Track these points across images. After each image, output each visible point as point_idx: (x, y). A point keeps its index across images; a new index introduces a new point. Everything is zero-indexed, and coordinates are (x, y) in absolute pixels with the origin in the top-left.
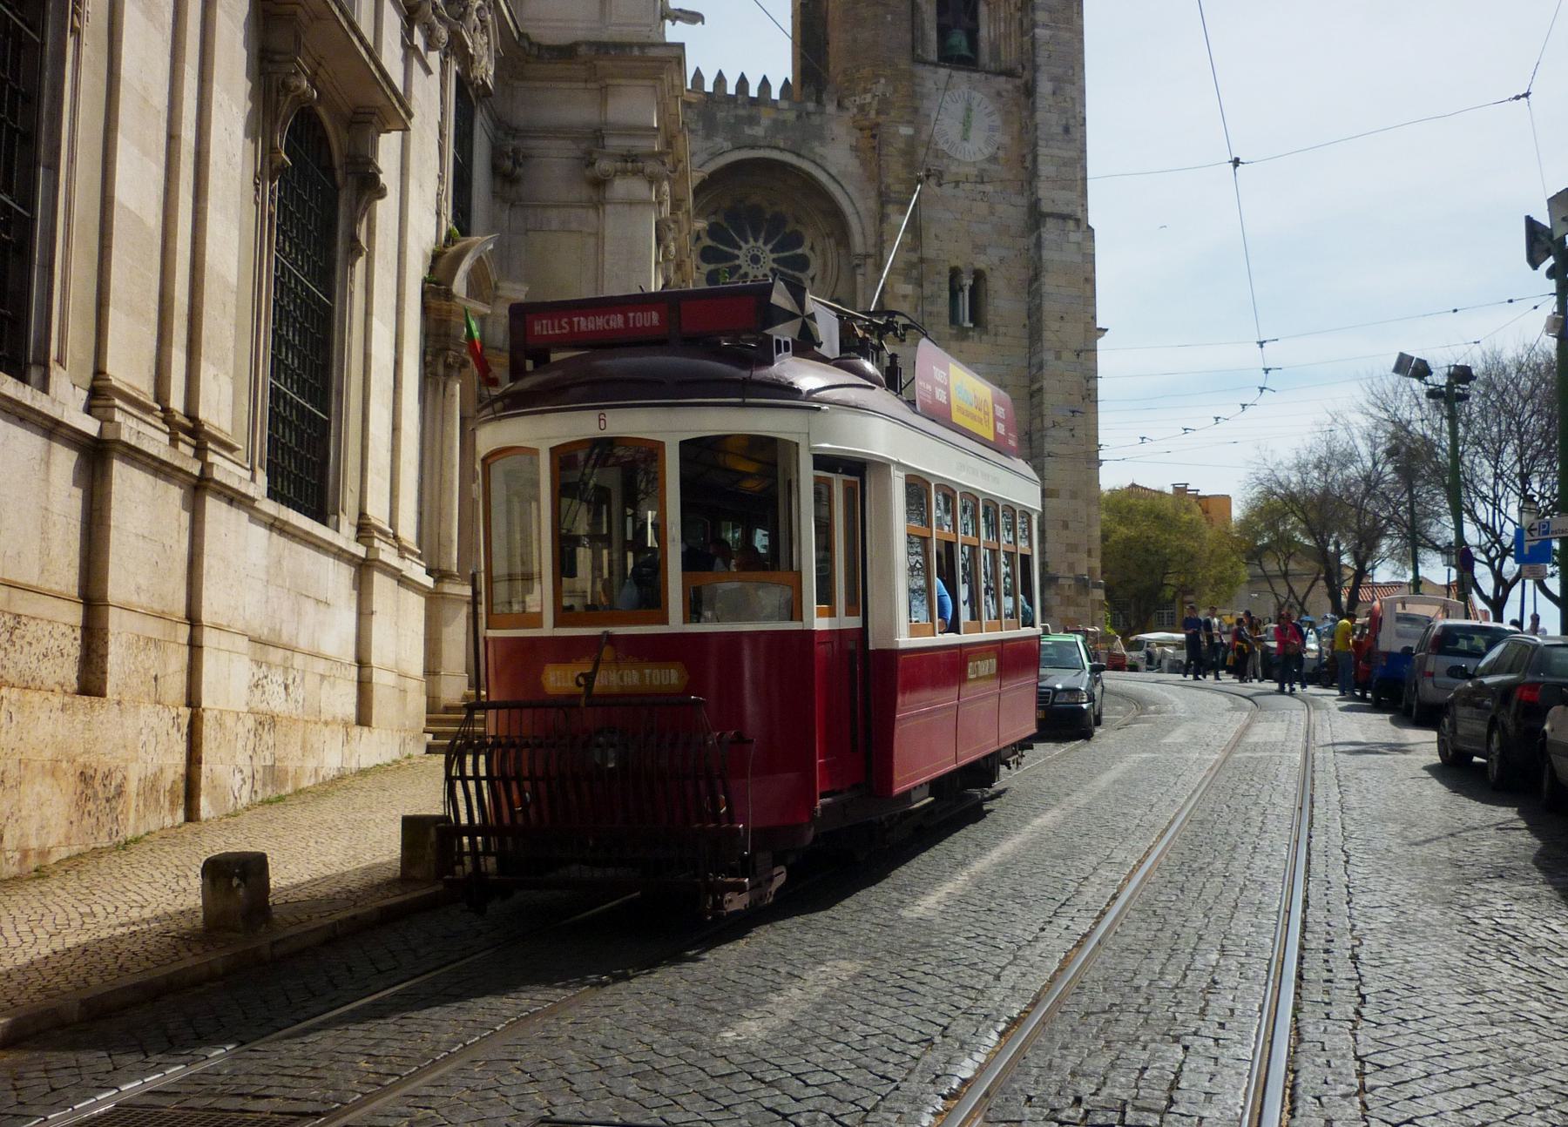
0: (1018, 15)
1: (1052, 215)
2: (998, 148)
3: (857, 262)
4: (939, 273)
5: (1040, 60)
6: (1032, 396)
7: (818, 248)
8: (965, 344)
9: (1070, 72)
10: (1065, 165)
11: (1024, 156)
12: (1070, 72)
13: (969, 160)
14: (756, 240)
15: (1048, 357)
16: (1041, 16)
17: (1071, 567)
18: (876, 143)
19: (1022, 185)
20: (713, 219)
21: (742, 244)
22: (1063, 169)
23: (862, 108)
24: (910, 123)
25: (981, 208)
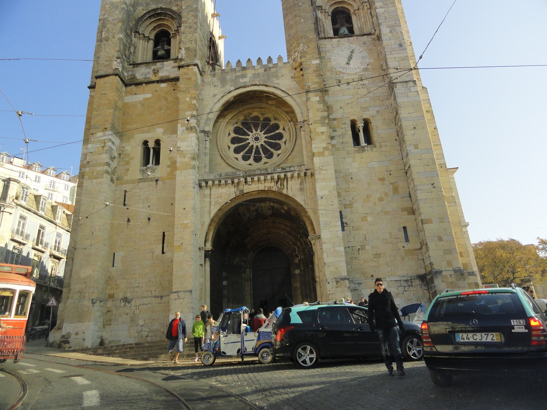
1: (397, 82)
2: (368, 65)
4: (344, 124)
5: (380, 21)
6: (406, 173)
7: (286, 129)
8: (364, 154)
9: (398, 22)
10: (402, 60)
12: (398, 22)
13: (353, 72)
14: (256, 131)
15: (410, 148)
17: (449, 263)
18: (301, 73)
20: (236, 125)
21: (250, 133)
22: (403, 61)
23: (294, 60)
25: (364, 91)
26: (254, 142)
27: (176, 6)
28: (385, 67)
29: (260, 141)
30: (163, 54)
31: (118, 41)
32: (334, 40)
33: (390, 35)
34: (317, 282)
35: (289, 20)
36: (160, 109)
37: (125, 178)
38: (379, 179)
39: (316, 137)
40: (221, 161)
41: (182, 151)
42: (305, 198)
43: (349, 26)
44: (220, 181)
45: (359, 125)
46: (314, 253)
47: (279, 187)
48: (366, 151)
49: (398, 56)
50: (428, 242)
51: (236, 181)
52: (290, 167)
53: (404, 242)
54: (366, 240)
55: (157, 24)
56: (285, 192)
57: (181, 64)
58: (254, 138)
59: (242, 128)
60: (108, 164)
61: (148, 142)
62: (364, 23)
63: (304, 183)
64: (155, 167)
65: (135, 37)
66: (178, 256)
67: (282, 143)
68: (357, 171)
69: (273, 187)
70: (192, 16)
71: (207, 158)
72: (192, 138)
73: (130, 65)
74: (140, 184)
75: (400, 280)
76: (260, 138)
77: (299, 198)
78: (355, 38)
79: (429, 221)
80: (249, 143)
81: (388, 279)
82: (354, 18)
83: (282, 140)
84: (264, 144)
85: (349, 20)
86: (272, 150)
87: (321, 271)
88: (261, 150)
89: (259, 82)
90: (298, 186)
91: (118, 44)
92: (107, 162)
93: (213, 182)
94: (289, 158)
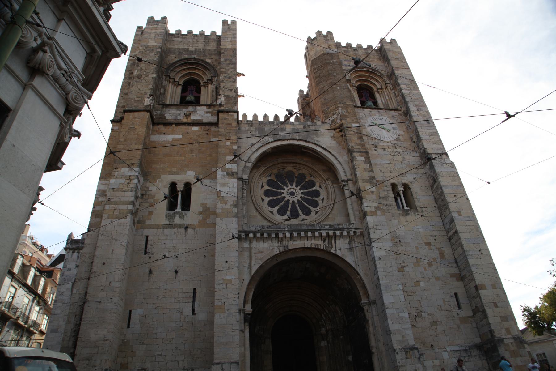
0: (393, 91)
2: (399, 135)
3: (343, 183)
4: (386, 186)
5: (407, 100)
8: (407, 217)
9: (422, 103)
10: (432, 135)
11: (411, 137)
12: (422, 103)
13: (387, 140)
14: (292, 185)
15: (455, 215)
16: (402, 86)
18: (342, 133)
19: (414, 148)
20: (269, 178)
21: (285, 187)
22: (433, 136)
24: (357, 122)
26: (289, 197)
27: (210, 58)
28: (414, 140)
29: (296, 197)
30: (192, 99)
31: (152, 80)
32: (365, 110)
33: (417, 113)
34: (373, 353)
35: (324, 87)
36: (191, 151)
37: (148, 222)
38: (425, 243)
39: (367, 196)
40: (257, 214)
41: (223, 197)
42: (355, 259)
43: (374, 101)
44: (262, 235)
45: (400, 189)
46: (368, 321)
47: (327, 245)
48: (410, 215)
49: (428, 131)
50: (486, 308)
51: (281, 235)
52: (339, 225)
53: (457, 309)
54: (421, 306)
55: (188, 72)
56: (333, 250)
57: (220, 109)
58: (289, 192)
59: (276, 182)
60: (133, 203)
61: (177, 185)
62: (388, 100)
63: (353, 243)
64: (184, 212)
65: (165, 80)
66: (219, 319)
67: (319, 200)
68: (404, 234)
69: (320, 245)
70: (231, 68)
71: (245, 207)
72: (233, 184)
73: (159, 105)
74: (165, 230)
75: (460, 350)
76: (296, 194)
77: (349, 259)
78: (385, 111)
79: (483, 287)
80: (284, 197)
81: (448, 349)
82: (377, 95)
83: (320, 197)
84: (300, 199)
85: (373, 97)
86: (310, 207)
87: (379, 341)
88: (297, 205)
89: (299, 137)
90: (347, 246)
91: (151, 83)
92: (132, 201)
93: (255, 235)
94: (329, 216)
